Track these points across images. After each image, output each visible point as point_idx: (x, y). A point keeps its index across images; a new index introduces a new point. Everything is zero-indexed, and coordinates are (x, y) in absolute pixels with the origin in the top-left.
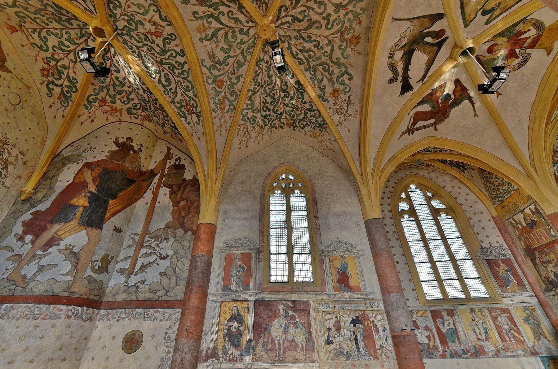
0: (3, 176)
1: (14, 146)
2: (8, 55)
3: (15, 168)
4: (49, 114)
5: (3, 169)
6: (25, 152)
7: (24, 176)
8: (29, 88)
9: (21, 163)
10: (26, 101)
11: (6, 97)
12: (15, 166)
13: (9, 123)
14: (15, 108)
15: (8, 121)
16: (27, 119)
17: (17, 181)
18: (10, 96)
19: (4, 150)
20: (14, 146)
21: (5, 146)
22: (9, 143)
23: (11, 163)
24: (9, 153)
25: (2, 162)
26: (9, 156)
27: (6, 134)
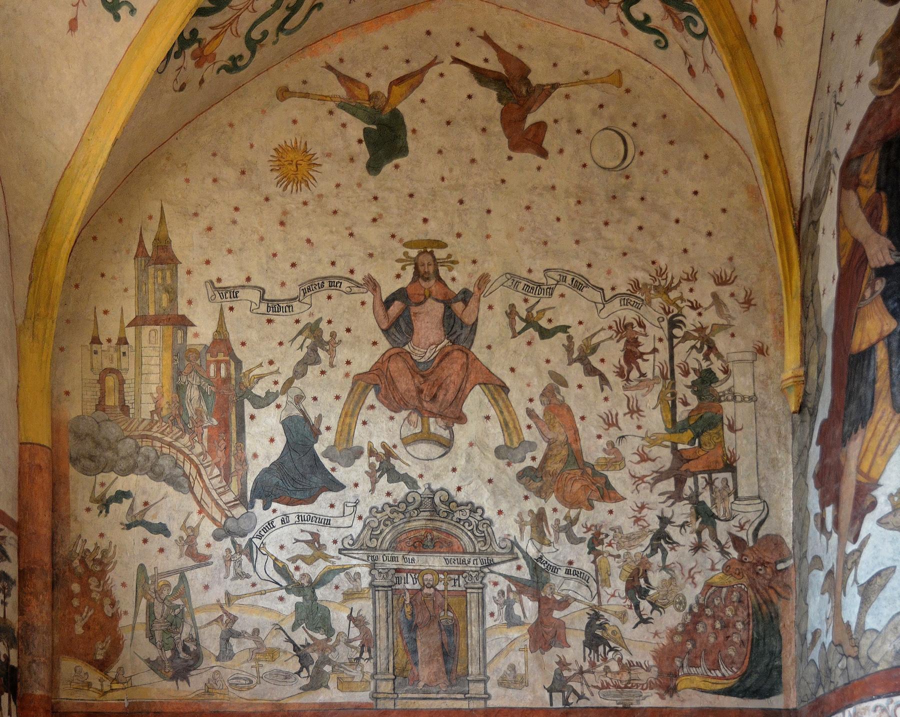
0: (720, 376)
1: (692, 277)
2: (520, 47)
3: (733, 335)
4: (709, 100)
5: (707, 357)
6: (729, 272)
7: (769, 341)
8: (616, 78)
9: (738, 307)
10: (634, 125)
11: (590, 163)
12: (730, 331)
13: (640, 228)
14: (627, 172)
15: (634, 222)
16: (673, 172)
17: (761, 367)
18: (596, 151)
19: (677, 307)
20: (692, 277)
21: (673, 295)
22: (676, 282)
23: (718, 328)
24: (695, 306)
25: (693, 342)
26: (700, 314)
27: (654, 263)
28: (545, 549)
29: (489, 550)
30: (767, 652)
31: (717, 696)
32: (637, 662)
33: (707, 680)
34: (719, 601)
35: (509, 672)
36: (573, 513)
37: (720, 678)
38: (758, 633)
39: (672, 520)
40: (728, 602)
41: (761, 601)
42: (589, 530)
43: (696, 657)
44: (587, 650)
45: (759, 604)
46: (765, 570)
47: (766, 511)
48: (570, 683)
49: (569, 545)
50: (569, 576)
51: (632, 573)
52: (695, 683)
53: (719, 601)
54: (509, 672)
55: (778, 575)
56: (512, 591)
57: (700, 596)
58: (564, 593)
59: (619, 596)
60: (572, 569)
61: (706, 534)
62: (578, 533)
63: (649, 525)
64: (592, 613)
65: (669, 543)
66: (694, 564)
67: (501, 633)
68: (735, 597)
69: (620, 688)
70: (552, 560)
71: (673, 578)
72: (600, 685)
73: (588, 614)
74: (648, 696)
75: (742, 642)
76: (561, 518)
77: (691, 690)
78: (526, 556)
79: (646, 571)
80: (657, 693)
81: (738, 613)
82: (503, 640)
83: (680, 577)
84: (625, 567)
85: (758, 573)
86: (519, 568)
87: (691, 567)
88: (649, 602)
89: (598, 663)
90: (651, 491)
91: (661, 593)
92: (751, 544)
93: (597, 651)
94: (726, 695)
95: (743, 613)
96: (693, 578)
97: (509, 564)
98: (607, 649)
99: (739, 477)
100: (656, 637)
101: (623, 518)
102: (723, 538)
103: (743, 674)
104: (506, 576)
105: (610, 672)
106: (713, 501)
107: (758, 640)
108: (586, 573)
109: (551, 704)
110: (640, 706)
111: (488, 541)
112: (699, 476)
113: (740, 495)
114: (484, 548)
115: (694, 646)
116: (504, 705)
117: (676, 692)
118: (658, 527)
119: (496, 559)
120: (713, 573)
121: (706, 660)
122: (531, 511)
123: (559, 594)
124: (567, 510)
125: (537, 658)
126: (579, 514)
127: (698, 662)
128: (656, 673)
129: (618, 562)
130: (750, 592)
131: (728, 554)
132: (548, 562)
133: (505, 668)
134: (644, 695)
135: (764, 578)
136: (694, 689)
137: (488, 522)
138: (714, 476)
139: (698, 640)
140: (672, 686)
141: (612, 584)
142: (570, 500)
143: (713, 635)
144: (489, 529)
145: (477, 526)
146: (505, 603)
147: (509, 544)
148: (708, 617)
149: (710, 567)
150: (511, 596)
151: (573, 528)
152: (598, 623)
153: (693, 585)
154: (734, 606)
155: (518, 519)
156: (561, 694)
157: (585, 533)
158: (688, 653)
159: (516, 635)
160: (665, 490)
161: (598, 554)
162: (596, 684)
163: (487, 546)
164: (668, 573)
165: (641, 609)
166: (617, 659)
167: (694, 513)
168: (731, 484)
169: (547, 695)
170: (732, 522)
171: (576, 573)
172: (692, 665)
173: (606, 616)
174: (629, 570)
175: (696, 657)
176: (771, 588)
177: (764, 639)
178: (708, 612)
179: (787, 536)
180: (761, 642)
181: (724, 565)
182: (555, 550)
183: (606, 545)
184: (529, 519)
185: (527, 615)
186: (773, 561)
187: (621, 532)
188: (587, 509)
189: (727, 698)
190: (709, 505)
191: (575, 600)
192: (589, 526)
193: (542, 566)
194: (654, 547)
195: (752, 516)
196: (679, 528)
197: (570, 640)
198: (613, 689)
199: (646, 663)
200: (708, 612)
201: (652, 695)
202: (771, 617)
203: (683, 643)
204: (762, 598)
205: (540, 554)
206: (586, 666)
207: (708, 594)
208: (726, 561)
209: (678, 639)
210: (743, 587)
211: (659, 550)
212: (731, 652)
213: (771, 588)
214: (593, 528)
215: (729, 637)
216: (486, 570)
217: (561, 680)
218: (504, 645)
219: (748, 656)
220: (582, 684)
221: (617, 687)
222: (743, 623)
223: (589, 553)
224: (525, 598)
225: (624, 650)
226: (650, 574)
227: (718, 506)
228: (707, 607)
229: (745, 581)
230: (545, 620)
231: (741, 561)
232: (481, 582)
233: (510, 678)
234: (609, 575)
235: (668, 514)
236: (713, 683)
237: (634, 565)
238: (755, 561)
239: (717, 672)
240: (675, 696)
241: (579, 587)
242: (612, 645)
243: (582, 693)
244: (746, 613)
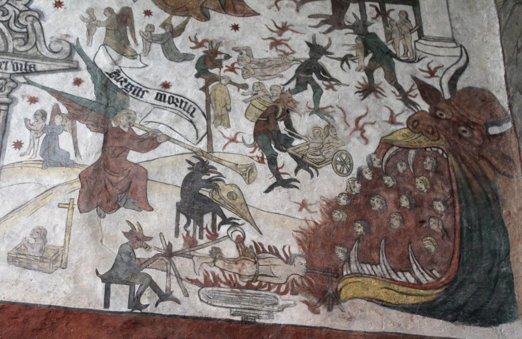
28: (125, 62)
29: (30, 52)
30: (486, 251)
31: (409, 315)
32: (269, 247)
33: (392, 286)
34: (404, 168)
35: (32, 241)
36: (176, 21)
37: (413, 286)
38: (468, 221)
39: (329, 50)
40: (418, 170)
41: (470, 175)
42: (199, 45)
43: (371, 248)
44: (183, 219)
45: (467, 179)
46: (472, 132)
47: (464, 58)
48: (146, 271)
49: (166, 60)
50: (162, 103)
51: (264, 113)
52: (371, 291)
53: (404, 168)
54: (32, 241)
55: (491, 143)
56: (59, 113)
57: (374, 157)
58: (151, 126)
59: (244, 142)
60: (168, 95)
61: (379, 75)
62: (181, 47)
63: (294, 52)
64: (195, 161)
65: (326, 79)
66: (364, 112)
67: (29, 175)
68: (429, 163)
69: (240, 287)
70: (134, 79)
71: (330, 126)
72: (201, 279)
73: (189, 162)
74: (288, 306)
75: (445, 231)
76: (157, 25)
77: (364, 302)
78: (92, 67)
79: (288, 111)
80: (305, 302)
81: (436, 187)
82: (32, 187)
83: (342, 126)
84: (255, 102)
85: (460, 136)
86: (78, 82)
87: (360, 115)
88: (292, 156)
89: (200, 242)
90: (298, 10)
91: (312, 145)
92: (447, 95)
93: (200, 222)
94: (424, 315)
95: (443, 189)
96: (363, 131)
97: (61, 75)
98: (219, 220)
99: (423, 14)
100: (304, 210)
101: (255, 38)
102: (406, 84)
103: (451, 283)
104: (53, 92)
105: (222, 258)
106: (389, 35)
107: (470, 231)
108: (190, 103)
109: (107, 304)
110: (274, 322)
111: (32, 39)
112: (367, 4)
113: (426, 33)
114: (23, 49)
115: (368, 230)
116: (13, 299)
117: (338, 303)
118: (308, 57)
119: (40, 66)
120: (394, 128)
121: (388, 254)
122: (109, 10)
123: (141, 127)
124: (167, 15)
125: (90, 222)
126: (185, 23)
127: (375, 255)
128: (304, 267)
129: (243, 94)
130: (451, 159)
131: (415, 104)
132: (129, 81)
133: (26, 233)
134: (281, 303)
135: (471, 143)
136: (370, 300)
137: (36, 15)
138: (388, 7)
139: (374, 222)
140: (330, 291)
141: (232, 123)
142: (173, 4)
143: (398, 217)
144: (36, 25)
145: (17, 18)
146: (44, 129)
147: (67, 48)
148: (388, 189)
149: (388, 119)
150: (58, 120)
151: (175, 40)
152: (205, 177)
153: (363, 141)
154: (428, 177)
155: (86, 16)
156: (127, 288)
157: (192, 48)
158: (359, 239)
159: (56, 182)
160: (317, 12)
161: (212, 79)
162: (194, 277)
163: (28, 47)
164: (322, 118)
165: (280, 164)
166: (234, 238)
167: (361, 45)
168: (412, 18)
169: (101, 286)
170: (418, 65)
171: (173, 100)
172: (364, 259)
173: (220, 169)
174: (261, 106)
175: (371, 248)
176: (483, 157)
177: (480, 231)
178: (388, 180)
179: (498, 92)
180: (476, 235)
181: (409, 118)
182: (141, 65)
183: (225, 68)
184: (104, 19)
185: (82, 150)
186: (481, 122)
187: (250, 55)
188: (199, 18)
189: (427, 320)
190: (383, 39)
191: (169, 139)
192: (200, 40)
193: (118, 84)
194: (300, 81)
195: (446, 62)
196: (339, 62)
197: (153, 198)
198: (225, 289)
199: (286, 249)
200: (388, 180)
201: (295, 304)
202: (488, 199)
203: (349, 224)
204: (470, 171)
205: (116, 68)
206: (178, 245)
207: (387, 156)
208: (412, 113)
209: (339, 216)
210: (440, 151)
211: (309, 86)
212: (429, 245)
213: (483, 157)
214: (206, 44)
215: (423, 222)
216: (21, 79)
217: (129, 264)
218: (31, 196)
219: (456, 255)
220: (169, 274)
221: (232, 284)
222: (445, 203)
223: (197, 76)
224: (81, 127)
225: (247, 224)
226: (294, 117)
227: (396, 41)
228: (387, 174)
229: (442, 143)
230: (112, 163)
231: (434, 115)
232: (8, 96)
233: (34, 252)
234: (229, 110)
235: (322, 41)
236: (401, 293)
237: (269, 102)
238: (454, 119)
239: (408, 275)
240: (336, 310)
241: (177, 121)
242: (228, 214)
243: (168, 289)
244: (447, 190)
